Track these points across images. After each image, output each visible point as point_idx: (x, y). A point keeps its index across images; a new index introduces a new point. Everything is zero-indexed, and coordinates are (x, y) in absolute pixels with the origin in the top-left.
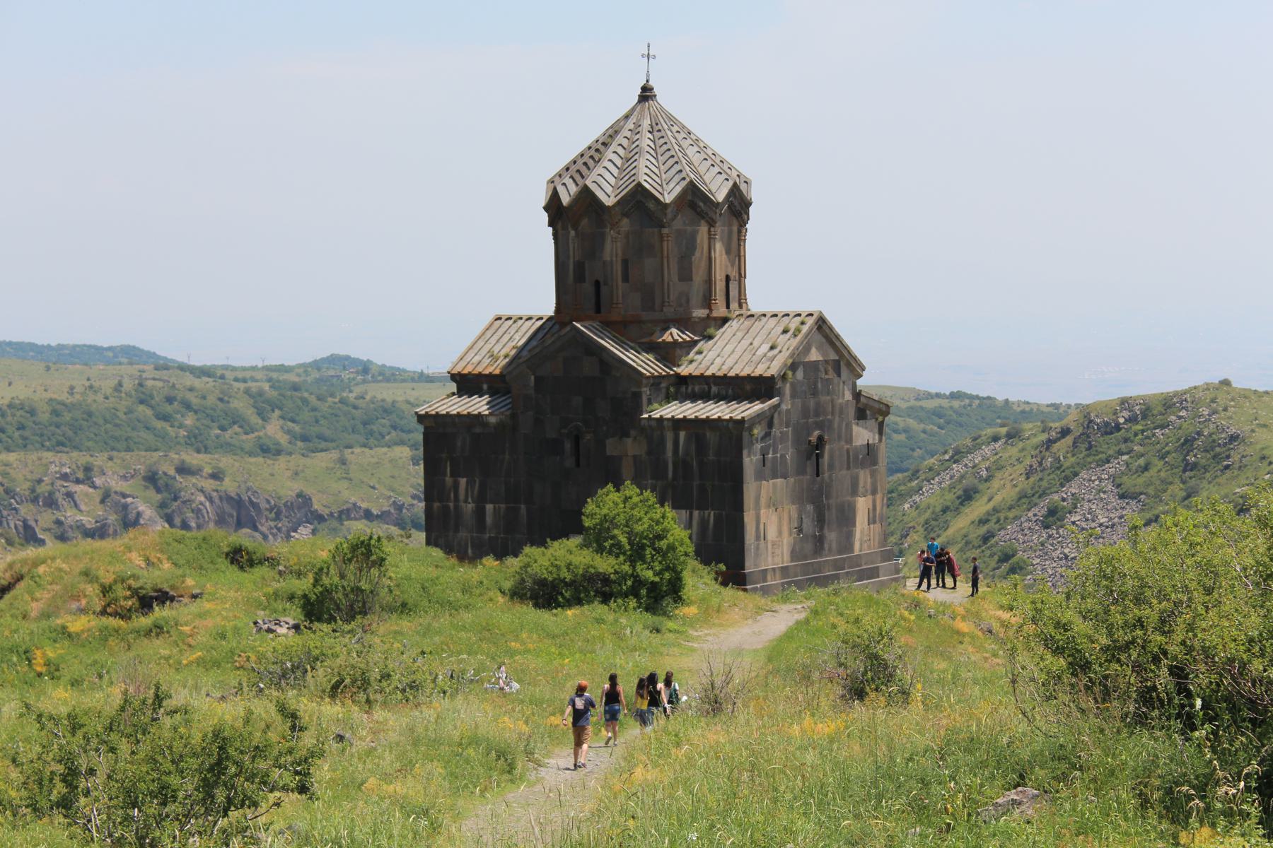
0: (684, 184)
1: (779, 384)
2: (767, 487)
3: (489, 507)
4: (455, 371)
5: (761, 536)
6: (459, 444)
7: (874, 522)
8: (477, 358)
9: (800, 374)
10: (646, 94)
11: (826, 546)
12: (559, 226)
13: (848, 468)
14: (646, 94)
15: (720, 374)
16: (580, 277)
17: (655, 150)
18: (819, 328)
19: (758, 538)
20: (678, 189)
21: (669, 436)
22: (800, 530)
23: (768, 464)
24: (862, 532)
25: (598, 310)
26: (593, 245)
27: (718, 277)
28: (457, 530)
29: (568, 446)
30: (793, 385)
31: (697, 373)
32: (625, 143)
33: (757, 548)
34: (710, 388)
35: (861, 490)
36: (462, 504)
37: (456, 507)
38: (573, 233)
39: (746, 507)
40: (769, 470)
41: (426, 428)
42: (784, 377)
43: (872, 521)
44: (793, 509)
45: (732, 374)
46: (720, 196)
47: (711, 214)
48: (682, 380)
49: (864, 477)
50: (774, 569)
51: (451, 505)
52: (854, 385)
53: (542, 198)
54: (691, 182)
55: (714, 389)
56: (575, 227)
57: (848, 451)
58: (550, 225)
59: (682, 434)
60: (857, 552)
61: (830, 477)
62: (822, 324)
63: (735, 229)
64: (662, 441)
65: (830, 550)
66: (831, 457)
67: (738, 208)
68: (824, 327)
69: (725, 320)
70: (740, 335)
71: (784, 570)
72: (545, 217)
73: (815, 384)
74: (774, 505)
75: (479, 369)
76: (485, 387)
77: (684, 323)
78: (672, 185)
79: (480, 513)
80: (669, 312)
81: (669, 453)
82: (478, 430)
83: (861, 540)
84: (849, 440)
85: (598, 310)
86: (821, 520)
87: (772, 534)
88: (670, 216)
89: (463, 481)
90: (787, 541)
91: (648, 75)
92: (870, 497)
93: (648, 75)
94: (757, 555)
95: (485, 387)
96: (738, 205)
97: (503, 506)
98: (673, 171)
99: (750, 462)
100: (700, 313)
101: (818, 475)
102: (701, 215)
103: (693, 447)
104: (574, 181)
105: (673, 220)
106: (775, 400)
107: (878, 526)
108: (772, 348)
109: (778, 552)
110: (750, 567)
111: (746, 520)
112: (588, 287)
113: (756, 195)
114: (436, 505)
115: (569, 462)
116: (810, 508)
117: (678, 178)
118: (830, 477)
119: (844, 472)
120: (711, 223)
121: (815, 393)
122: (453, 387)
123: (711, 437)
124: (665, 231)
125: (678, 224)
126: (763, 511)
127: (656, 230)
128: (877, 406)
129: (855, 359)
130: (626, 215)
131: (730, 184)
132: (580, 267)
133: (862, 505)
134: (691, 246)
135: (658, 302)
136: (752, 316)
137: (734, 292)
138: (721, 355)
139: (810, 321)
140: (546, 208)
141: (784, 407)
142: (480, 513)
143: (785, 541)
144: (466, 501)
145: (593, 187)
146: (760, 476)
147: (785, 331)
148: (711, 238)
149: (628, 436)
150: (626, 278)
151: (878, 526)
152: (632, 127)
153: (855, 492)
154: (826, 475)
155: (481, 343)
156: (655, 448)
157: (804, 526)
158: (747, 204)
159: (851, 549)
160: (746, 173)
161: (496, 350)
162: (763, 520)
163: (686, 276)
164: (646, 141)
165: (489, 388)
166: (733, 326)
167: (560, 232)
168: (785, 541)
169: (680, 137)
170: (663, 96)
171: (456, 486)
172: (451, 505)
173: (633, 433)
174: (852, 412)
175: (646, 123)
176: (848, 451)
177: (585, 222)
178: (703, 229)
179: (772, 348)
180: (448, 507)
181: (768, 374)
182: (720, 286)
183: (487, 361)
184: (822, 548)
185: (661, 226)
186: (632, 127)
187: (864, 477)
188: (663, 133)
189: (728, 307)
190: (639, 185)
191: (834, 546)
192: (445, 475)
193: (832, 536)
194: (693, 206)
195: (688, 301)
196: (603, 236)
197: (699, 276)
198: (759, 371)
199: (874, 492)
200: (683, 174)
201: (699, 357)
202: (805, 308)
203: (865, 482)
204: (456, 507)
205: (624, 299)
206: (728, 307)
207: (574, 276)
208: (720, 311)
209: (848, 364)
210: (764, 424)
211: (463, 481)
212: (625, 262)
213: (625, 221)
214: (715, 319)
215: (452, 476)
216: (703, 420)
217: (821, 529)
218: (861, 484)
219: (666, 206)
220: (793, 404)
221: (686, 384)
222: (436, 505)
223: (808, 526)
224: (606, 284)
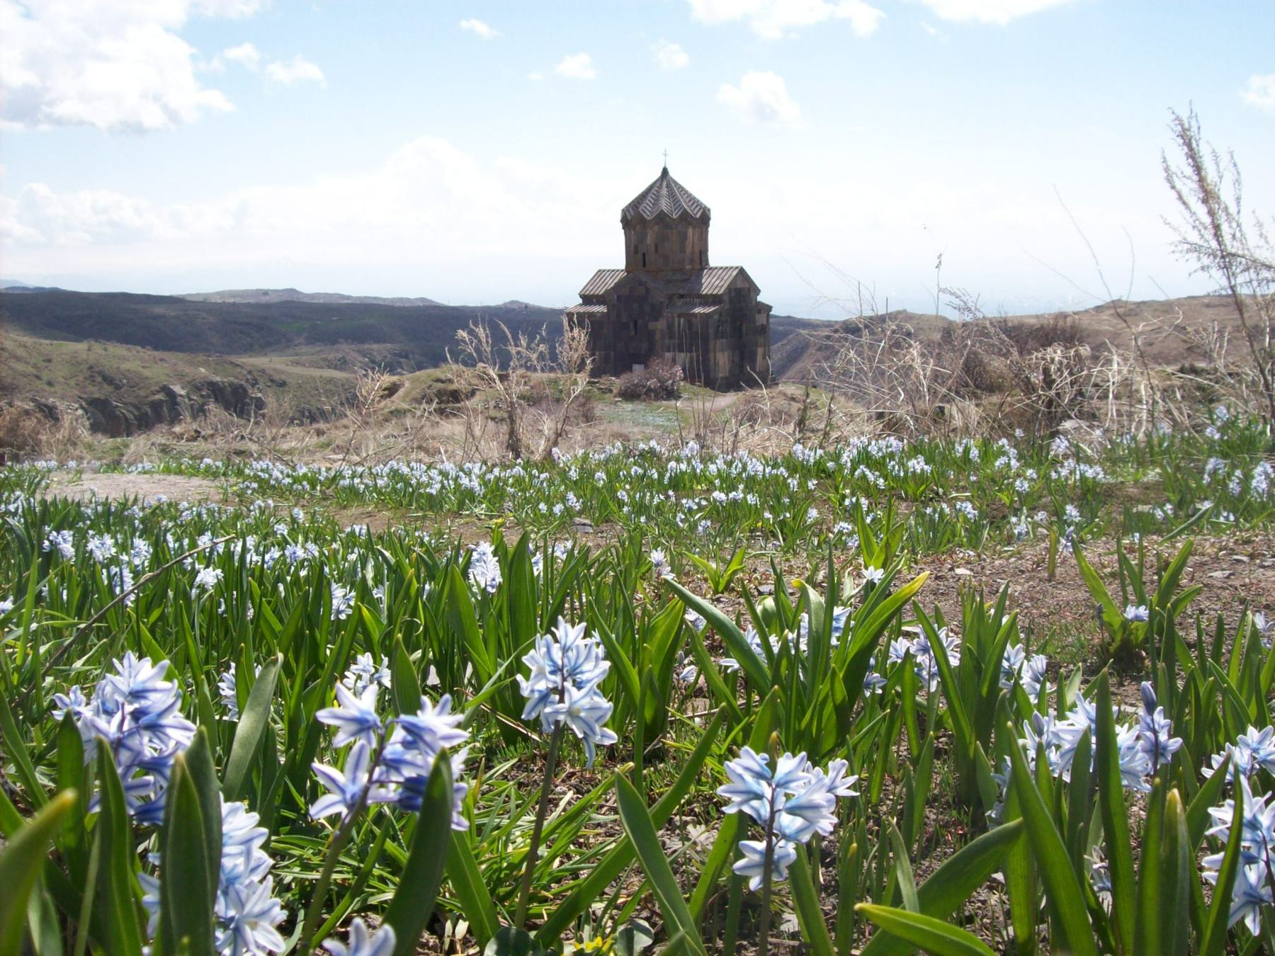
2: (719, 342)
5: (716, 364)
10: (665, 172)
14: (665, 172)
16: (636, 251)
29: (632, 325)
49: (761, 340)
53: (619, 217)
74: (722, 351)
86: (742, 358)
87: (721, 363)
96: (704, 219)
100: (688, 267)
102: (690, 223)
112: (640, 256)
113: (713, 215)
115: (633, 333)
120: (694, 228)
122: (581, 301)
132: (636, 248)
133: (760, 351)
134: (684, 237)
146: (716, 338)
150: (656, 251)
153: (756, 345)
160: (708, 206)
163: (683, 251)
164: (664, 191)
170: (672, 174)
177: (638, 227)
182: (697, 255)
187: (761, 340)
202: (735, 264)
207: (633, 251)
212: (656, 245)
223: (736, 359)
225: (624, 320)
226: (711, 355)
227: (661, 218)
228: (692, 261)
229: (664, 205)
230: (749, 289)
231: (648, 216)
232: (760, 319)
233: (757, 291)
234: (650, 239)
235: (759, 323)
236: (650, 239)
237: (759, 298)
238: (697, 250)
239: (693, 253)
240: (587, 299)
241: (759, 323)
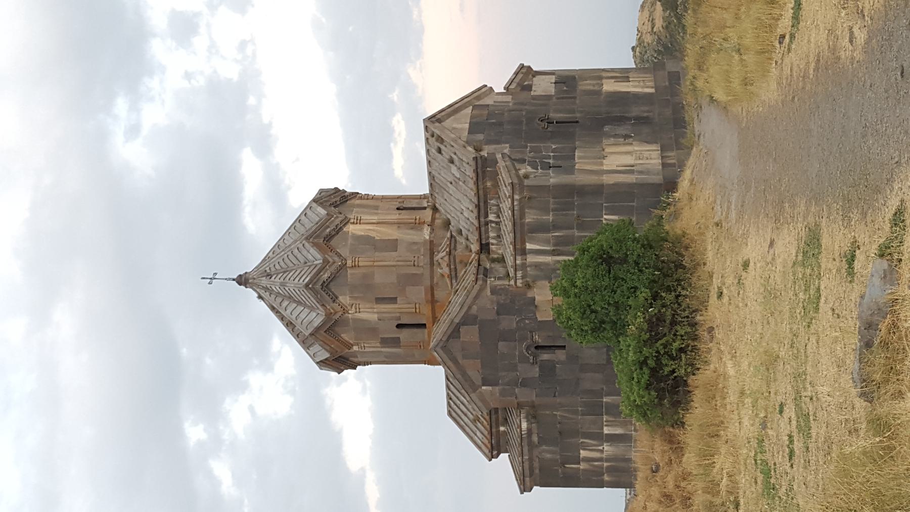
0: (307, 244)
1: (484, 154)
3: (606, 430)
4: (490, 455)
5: (629, 170)
6: (549, 456)
7: (628, 77)
8: (478, 434)
9: (480, 137)
10: (242, 280)
11: (645, 115)
12: (355, 360)
13: (575, 98)
14: (242, 280)
15: (476, 211)
16: (395, 342)
17: (285, 272)
18: (439, 121)
19: (631, 172)
20: (312, 250)
21: (531, 259)
22: (626, 137)
23: (559, 163)
24: (635, 87)
25: (423, 326)
26: (368, 330)
27: (397, 216)
28: (629, 460)
29: (545, 356)
30: (489, 142)
31: (477, 234)
32: (279, 300)
33: (641, 172)
34: (492, 222)
35: (596, 88)
36: (604, 456)
37: (607, 460)
38: (355, 348)
39: (599, 183)
40: (565, 163)
41: (537, 485)
42: (478, 150)
43: (627, 79)
44: (605, 142)
45: (475, 200)
46: (322, 212)
47: (337, 221)
48: (484, 248)
50: (662, 157)
51: (605, 464)
52: (499, 94)
54: (307, 239)
55: (492, 217)
56: (349, 346)
57: (558, 99)
58: (355, 368)
59: (529, 246)
60: (652, 90)
61: (581, 112)
62: (434, 120)
63: (358, 202)
64: (537, 266)
65: (648, 111)
66: (560, 112)
67: (338, 199)
68: (438, 116)
69: (435, 209)
70: (446, 195)
71: (663, 149)
72: (348, 373)
73: (493, 123)
75: (486, 433)
76: (502, 429)
77: (432, 248)
78: (310, 257)
79: (612, 438)
80: (424, 260)
81: (548, 259)
82: (535, 438)
83: (643, 87)
84: (549, 97)
85: (423, 326)
86: (621, 120)
87: (629, 160)
88: (336, 259)
89: (583, 453)
90: (637, 147)
91: (230, 279)
92: (604, 81)
93: (230, 279)
94: (647, 172)
95: (502, 429)
97: (605, 418)
98: (299, 256)
99: (554, 179)
100: (426, 233)
101: (577, 122)
102: (338, 230)
103: (541, 235)
104: (310, 346)
105: (340, 256)
106: (499, 156)
107: (630, 75)
108: (452, 161)
109: (646, 154)
110: (657, 179)
111: (611, 182)
112: (404, 334)
114: (606, 478)
115: (561, 355)
116: (607, 128)
117: (305, 252)
118: (581, 112)
119: (577, 102)
120: (346, 222)
121: (500, 124)
122: (504, 457)
123: (530, 217)
124: (349, 263)
125: (345, 252)
126: (605, 168)
127: (349, 271)
128: (520, 76)
129: (474, 92)
130: (335, 299)
131: (314, 205)
132: (385, 342)
133: (609, 86)
134: (367, 241)
135: (414, 271)
136: (431, 185)
137: (414, 204)
138: (460, 208)
139: (431, 127)
140: (340, 371)
141: (506, 151)
142: (612, 439)
143: (636, 148)
144: (602, 451)
145: (310, 331)
146: (571, 170)
147: (439, 151)
148: (359, 222)
149: (534, 299)
150: (393, 300)
151: (630, 75)
152: (268, 293)
153: (598, 93)
154: (578, 115)
155: (467, 429)
156: (546, 272)
157: (624, 132)
158: (336, 190)
159: (652, 94)
161: (471, 417)
162: (615, 168)
163: (392, 245)
165: (503, 425)
166: (439, 201)
167: (360, 359)
168: (636, 148)
169: (279, 251)
170: (250, 265)
171: (588, 460)
172: (605, 464)
173: (530, 295)
174: (524, 95)
175: (264, 281)
176: (558, 99)
178: (351, 228)
179: (452, 161)
180: (608, 467)
181: (473, 163)
182: (405, 216)
183: (479, 425)
184: (647, 117)
185: (343, 266)
186: (268, 293)
187: (586, 85)
188: (272, 266)
189: (425, 208)
190: (307, 286)
191: (646, 108)
192: (579, 469)
193: (635, 111)
194: (329, 238)
195: (415, 243)
196: (356, 320)
197: (392, 233)
198: (470, 172)
199: (601, 78)
200: (301, 246)
201: (464, 232)
203: (590, 84)
204: (607, 460)
205: (411, 303)
206: (425, 208)
208: (427, 215)
209: (478, 98)
210: (518, 166)
211: (583, 453)
212: (379, 300)
213: (341, 298)
214: (433, 219)
215: (579, 463)
216: (514, 224)
217: (629, 119)
218: (591, 88)
219: (326, 262)
220: (506, 143)
221: (488, 244)
222: (606, 478)
223: (621, 130)
224: (399, 318)
225: (535, 372)
226: (608, 180)
227: (323, 287)
228: (417, 225)
229: (296, 282)
230: (475, 107)
231: (316, 318)
232: (543, 87)
233: (484, 91)
234: (368, 313)
235: (552, 90)
236: (368, 313)
237: (499, 88)
238: (395, 216)
239: (399, 224)
240: (493, 450)
241: (552, 90)
